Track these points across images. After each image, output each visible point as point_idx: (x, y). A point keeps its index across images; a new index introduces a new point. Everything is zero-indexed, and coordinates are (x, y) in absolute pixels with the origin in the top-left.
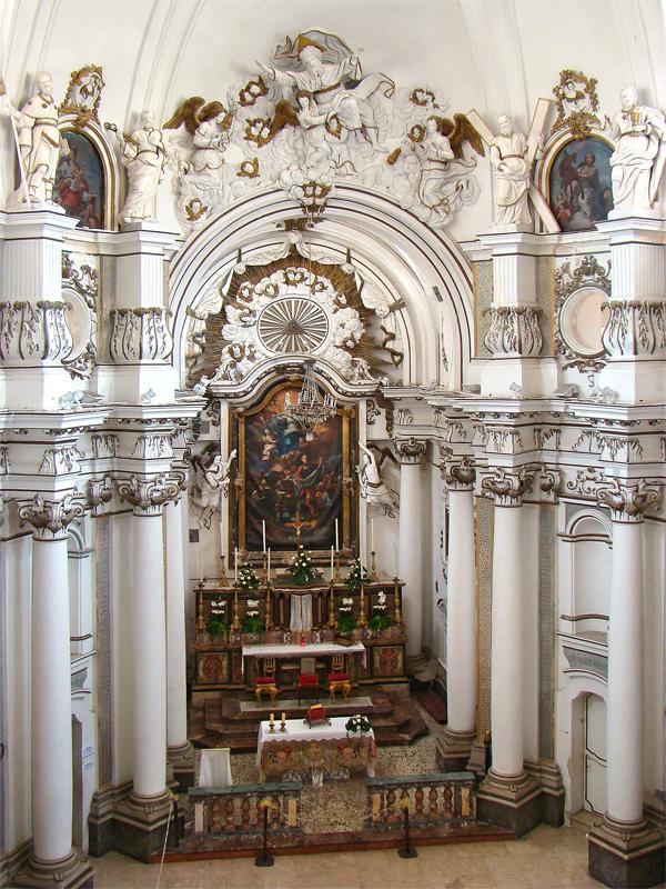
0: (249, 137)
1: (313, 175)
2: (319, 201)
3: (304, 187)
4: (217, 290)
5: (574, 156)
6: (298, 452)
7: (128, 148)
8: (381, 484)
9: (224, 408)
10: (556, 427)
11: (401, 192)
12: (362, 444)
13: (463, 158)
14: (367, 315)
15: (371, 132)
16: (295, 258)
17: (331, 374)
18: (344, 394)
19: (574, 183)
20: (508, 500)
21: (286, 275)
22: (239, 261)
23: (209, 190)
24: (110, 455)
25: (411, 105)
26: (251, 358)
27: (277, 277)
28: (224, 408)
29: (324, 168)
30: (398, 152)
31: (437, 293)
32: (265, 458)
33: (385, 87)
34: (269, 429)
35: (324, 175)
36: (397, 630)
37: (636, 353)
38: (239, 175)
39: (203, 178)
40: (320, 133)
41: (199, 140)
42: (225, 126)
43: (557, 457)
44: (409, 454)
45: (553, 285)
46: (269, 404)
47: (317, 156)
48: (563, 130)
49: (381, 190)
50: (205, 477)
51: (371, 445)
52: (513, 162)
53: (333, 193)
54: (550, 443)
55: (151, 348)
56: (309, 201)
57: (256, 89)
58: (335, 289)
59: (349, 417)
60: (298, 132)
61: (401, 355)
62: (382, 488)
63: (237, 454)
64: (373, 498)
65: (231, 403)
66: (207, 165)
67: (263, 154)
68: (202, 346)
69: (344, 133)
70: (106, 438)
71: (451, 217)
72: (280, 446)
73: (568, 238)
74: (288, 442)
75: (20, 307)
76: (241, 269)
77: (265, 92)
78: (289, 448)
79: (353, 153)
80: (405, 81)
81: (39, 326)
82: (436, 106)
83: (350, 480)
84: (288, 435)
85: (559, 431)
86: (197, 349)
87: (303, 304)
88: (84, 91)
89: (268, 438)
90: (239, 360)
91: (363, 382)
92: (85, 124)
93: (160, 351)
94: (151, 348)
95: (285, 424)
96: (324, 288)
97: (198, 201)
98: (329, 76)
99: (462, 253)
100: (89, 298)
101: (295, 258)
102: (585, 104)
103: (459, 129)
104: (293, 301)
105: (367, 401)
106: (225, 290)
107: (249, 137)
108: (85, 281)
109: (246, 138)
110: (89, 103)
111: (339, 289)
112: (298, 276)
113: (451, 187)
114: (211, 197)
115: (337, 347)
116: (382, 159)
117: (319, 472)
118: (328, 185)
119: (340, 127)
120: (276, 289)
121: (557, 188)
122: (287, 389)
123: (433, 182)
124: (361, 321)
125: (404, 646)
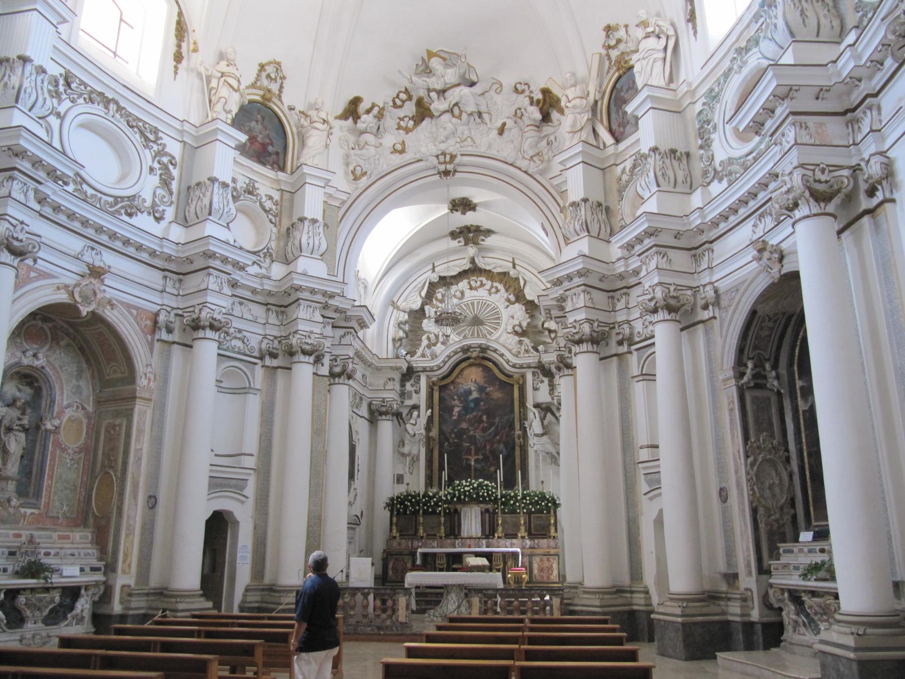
0: (399, 128)
1: (443, 147)
2: (450, 167)
3: (437, 156)
4: (417, 293)
6: (480, 413)
7: (302, 120)
8: (543, 435)
10: (625, 290)
12: (530, 404)
14: (531, 307)
15: (485, 116)
16: (474, 270)
17: (502, 350)
18: (514, 366)
20: (584, 347)
21: (469, 283)
22: (433, 271)
24: (279, 324)
25: (515, 95)
27: (463, 285)
29: (451, 142)
30: (504, 124)
31: (544, 229)
32: (455, 418)
33: (495, 87)
34: (459, 396)
35: (451, 147)
37: (658, 185)
38: (392, 153)
39: (364, 151)
40: (447, 116)
41: (361, 125)
42: (380, 116)
43: (629, 314)
45: (615, 187)
46: (457, 377)
48: (612, 71)
49: (493, 153)
50: (406, 430)
51: (537, 406)
52: (577, 102)
53: (458, 160)
54: (620, 305)
55: (308, 244)
56: (442, 168)
57: (403, 96)
58: (507, 291)
59: (518, 383)
60: (434, 122)
62: (545, 438)
63: (432, 413)
64: (539, 446)
65: (428, 376)
66: (366, 143)
67: (410, 139)
68: (405, 332)
69: (464, 116)
70: (277, 313)
71: (545, 164)
72: (466, 409)
73: (622, 146)
74: (472, 405)
75: (198, 184)
76: (435, 278)
77: (410, 98)
78: (473, 410)
79: (473, 132)
80: (508, 82)
81: (208, 194)
82: (531, 92)
83: (520, 432)
84: (472, 401)
85: (627, 294)
86: (401, 334)
87: (484, 304)
88: (268, 76)
89: (457, 402)
90: (435, 345)
91: (527, 355)
92: (269, 100)
93: (316, 247)
94: (308, 244)
95: (469, 392)
96: (498, 291)
100: (270, 217)
101: (474, 270)
103: (545, 100)
105: (533, 373)
106: (424, 293)
107: (399, 128)
108: (268, 205)
109: (398, 129)
110: (274, 87)
111: (511, 290)
112: (479, 283)
113: (544, 142)
115: (509, 333)
116: (496, 132)
117: (497, 428)
118: (454, 153)
120: (462, 293)
121: (613, 116)
122: (471, 365)
123: (529, 140)
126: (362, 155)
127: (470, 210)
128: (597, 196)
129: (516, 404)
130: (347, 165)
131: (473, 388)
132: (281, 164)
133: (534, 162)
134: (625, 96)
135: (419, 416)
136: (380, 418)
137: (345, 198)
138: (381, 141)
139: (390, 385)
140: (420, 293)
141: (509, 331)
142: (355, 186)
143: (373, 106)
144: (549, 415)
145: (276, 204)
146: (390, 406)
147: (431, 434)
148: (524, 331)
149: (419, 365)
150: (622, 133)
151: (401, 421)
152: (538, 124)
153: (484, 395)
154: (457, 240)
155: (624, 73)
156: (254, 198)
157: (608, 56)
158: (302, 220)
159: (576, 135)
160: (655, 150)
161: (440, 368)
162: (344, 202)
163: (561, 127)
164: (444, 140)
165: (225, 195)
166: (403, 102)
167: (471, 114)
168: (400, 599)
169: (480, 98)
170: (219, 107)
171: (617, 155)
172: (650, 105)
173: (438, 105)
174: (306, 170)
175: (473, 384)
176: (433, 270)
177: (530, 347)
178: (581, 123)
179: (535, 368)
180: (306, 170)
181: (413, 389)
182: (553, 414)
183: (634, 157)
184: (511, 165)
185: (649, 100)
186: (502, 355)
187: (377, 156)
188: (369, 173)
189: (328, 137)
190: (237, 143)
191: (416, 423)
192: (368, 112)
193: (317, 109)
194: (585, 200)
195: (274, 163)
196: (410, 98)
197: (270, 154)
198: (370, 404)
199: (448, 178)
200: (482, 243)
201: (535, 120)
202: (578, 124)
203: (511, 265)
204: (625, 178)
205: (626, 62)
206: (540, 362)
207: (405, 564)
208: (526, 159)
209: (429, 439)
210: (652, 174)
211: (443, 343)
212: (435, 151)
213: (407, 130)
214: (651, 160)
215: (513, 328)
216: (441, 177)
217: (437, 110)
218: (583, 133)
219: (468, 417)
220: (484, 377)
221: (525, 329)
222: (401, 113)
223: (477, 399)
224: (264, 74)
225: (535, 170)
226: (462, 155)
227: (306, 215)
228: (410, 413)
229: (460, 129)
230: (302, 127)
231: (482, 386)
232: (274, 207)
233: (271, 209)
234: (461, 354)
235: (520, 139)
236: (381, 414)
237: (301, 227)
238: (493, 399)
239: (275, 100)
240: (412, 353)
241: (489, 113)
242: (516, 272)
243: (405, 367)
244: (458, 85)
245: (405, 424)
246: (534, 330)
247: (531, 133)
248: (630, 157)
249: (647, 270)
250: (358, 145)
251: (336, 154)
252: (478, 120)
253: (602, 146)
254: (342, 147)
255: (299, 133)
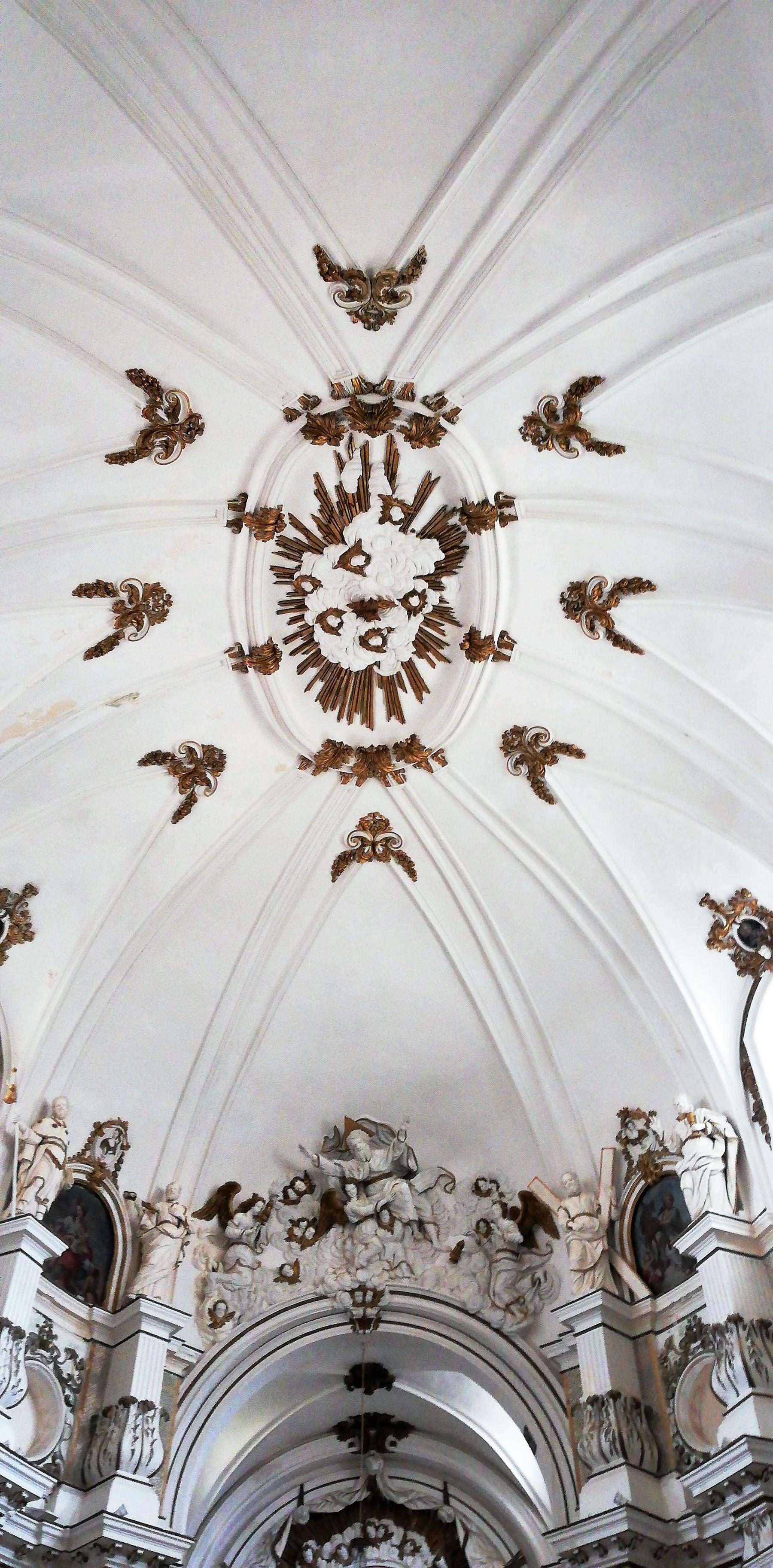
0: (291, 1237)
1: (362, 1276)
2: (371, 1312)
3: (352, 1292)
4: (268, 1549)
5: (652, 1205)
7: (145, 1217)
11: (469, 1295)
13: (537, 1247)
15: (430, 1228)
19: (658, 1236)
22: (300, 1499)
23: (237, 1290)
25: (476, 1198)
29: (376, 1269)
30: (461, 1245)
33: (443, 1181)
37: (752, 1384)
38: (276, 1280)
39: (234, 1276)
40: (370, 1226)
41: (232, 1231)
42: (262, 1218)
45: (658, 1372)
47: (367, 1254)
48: (634, 1178)
49: (443, 1292)
55: (133, 1451)
56: (358, 1312)
57: (300, 1185)
58: (432, 1550)
60: (347, 1232)
66: (238, 1261)
67: (307, 1256)
69: (398, 1227)
73: (664, 1301)
77: (311, 1189)
82: (501, 1195)
92: (100, 1182)
93: (144, 1460)
94: (133, 1451)
96: (416, 1550)
97: (223, 1301)
98: (378, 1161)
99: (546, 1361)
100: (68, 1392)
102: (649, 1142)
107: (291, 1237)
108: (68, 1368)
109: (287, 1240)
110: (110, 1161)
112: (382, 1531)
114: (240, 1299)
116: (444, 1257)
118: (380, 1289)
119: (393, 1219)
121: (643, 1249)
123: (503, 1276)
126: (229, 1282)
127: (381, 1386)
128: (630, 1389)
130: (202, 1297)
132: (99, 1292)
133: (513, 1313)
134: (660, 1219)
137: (194, 1361)
138: (259, 1258)
142: (211, 1338)
143: (255, 1198)
145: (80, 1366)
150: (662, 1279)
152: (515, 1249)
154: (349, 1441)
155: (655, 1183)
156: (47, 1354)
157: (626, 1152)
158: (126, 1402)
159: (586, 1276)
160: (736, 1320)
162: (189, 1368)
163: (553, 1256)
164: (365, 1264)
165: (14, 1353)
166: (300, 1194)
167: (408, 1224)
169: (422, 1199)
170: (30, 1194)
171: (655, 1316)
172: (715, 1244)
173: (357, 1206)
174: (145, 1307)
176: (300, 1499)
178: (592, 1256)
180: (145, 1307)
183: (685, 1322)
184: (473, 1316)
185: (712, 1236)
187: (254, 1286)
188: (237, 1315)
189: (182, 1248)
190: (47, 1256)
192: (245, 1207)
193: (169, 1201)
194: (614, 1395)
195: (89, 1290)
196: (311, 1189)
197: (85, 1274)
199: (367, 1331)
200: (392, 1449)
201: (511, 1242)
202: (589, 1259)
203: (439, 1496)
204: (673, 1357)
205: (657, 1166)
208: (499, 1308)
210: (738, 1363)
212: (348, 1282)
213: (304, 1243)
214: (732, 1338)
216: (354, 1329)
217: (356, 1214)
218: (597, 1273)
222: (296, 1213)
224: (99, 1140)
225: (515, 1328)
226: (392, 1292)
227: (133, 1394)
229: (391, 1247)
230: (143, 1228)
232: (76, 1373)
233: (70, 1377)
235: (486, 1270)
237: (122, 1416)
239: (108, 1182)
241: (435, 1224)
242: (451, 1511)
244: (387, 1175)
247: (505, 1264)
248: (679, 1321)
249: (755, 1545)
250: (224, 1264)
251: (189, 1275)
252: (420, 1236)
253: (627, 1297)
254: (196, 1266)
255: (135, 1237)
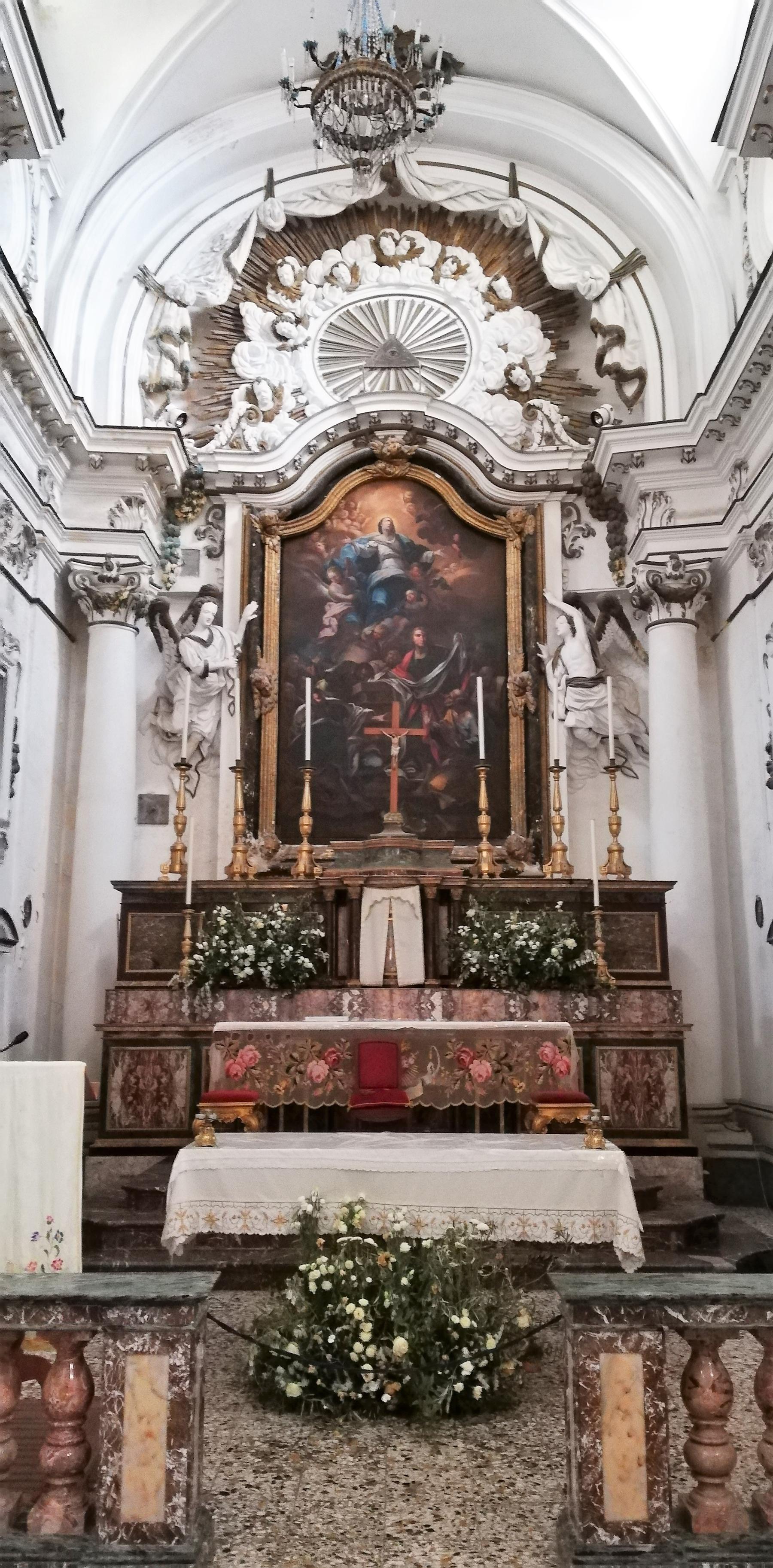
4: (220, 258)
6: (404, 621)
8: (598, 680)
9: (234, 516)
12: (553, 593)
21: (376, 245)
22: (269, 190)
26: (299, 414)
28: (234, 516)
32: (328, 633)
34: (339, 569)
36: (660, 1005)
44: (668, 597)
51: (574, 600)
58: (486, 271)
59: (520, 533)
61: (640, 375)
62: (605, 692)
64: (581, 716)
65: (250, 508)
68: (183, 369)
74: (380, 598)
78: (382, 612)
89: (335, 588)
95: (371, 561)
96: (461, 271)
104: (392, 301)
105: (564, 505)
106: (239, 259)
112: (405, 244)
115: (492, 392)
120: (354, 270)
124: (546, 336)
125: (679, 1044)
129: (513, 593)
131: (383, 550)
135: (218, 620)
136: (97, 617)
139: (130, 518)
140: (227, 255)
141: (492, 386)
144: (613, 625)
146: (131, 581)
147: (256, 675)
148: (536, 387)
149: (222, 468)
151: (164, 632)
153: (415, 569)
161: (285, 484)
168: (133, 1368)
175: (383, 538)
176: (269, 190)
177: (558, 428)
179: (570, 490)
181: (202, 545)
182: (625, 625)
186: (472, 451)
191: (211, 637)
198: (64, 575)
203: (504, 187)
206: (589, 469)
207: (169, 1072)
209: (250, 689)
211: (292, 414)
215: (508, 373)
219: (367, 630)
220: (419, 519)
221: (539, 380)
223: (393, 580)
228: (194, 611)
231: (411, 544)
234: (349, 445)
236: (100, 604)
238: (443, 583)
240: (204, 439)
243: (178, 468)
245: (176, 641)
246: (567, 384)
